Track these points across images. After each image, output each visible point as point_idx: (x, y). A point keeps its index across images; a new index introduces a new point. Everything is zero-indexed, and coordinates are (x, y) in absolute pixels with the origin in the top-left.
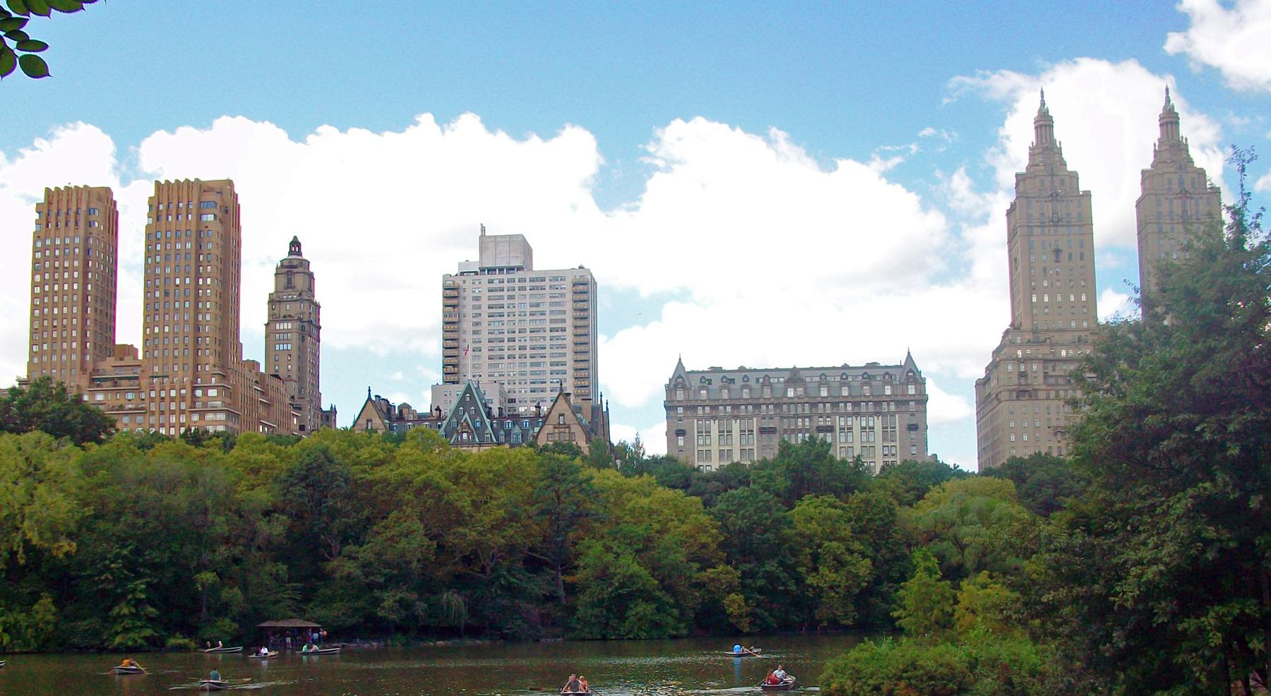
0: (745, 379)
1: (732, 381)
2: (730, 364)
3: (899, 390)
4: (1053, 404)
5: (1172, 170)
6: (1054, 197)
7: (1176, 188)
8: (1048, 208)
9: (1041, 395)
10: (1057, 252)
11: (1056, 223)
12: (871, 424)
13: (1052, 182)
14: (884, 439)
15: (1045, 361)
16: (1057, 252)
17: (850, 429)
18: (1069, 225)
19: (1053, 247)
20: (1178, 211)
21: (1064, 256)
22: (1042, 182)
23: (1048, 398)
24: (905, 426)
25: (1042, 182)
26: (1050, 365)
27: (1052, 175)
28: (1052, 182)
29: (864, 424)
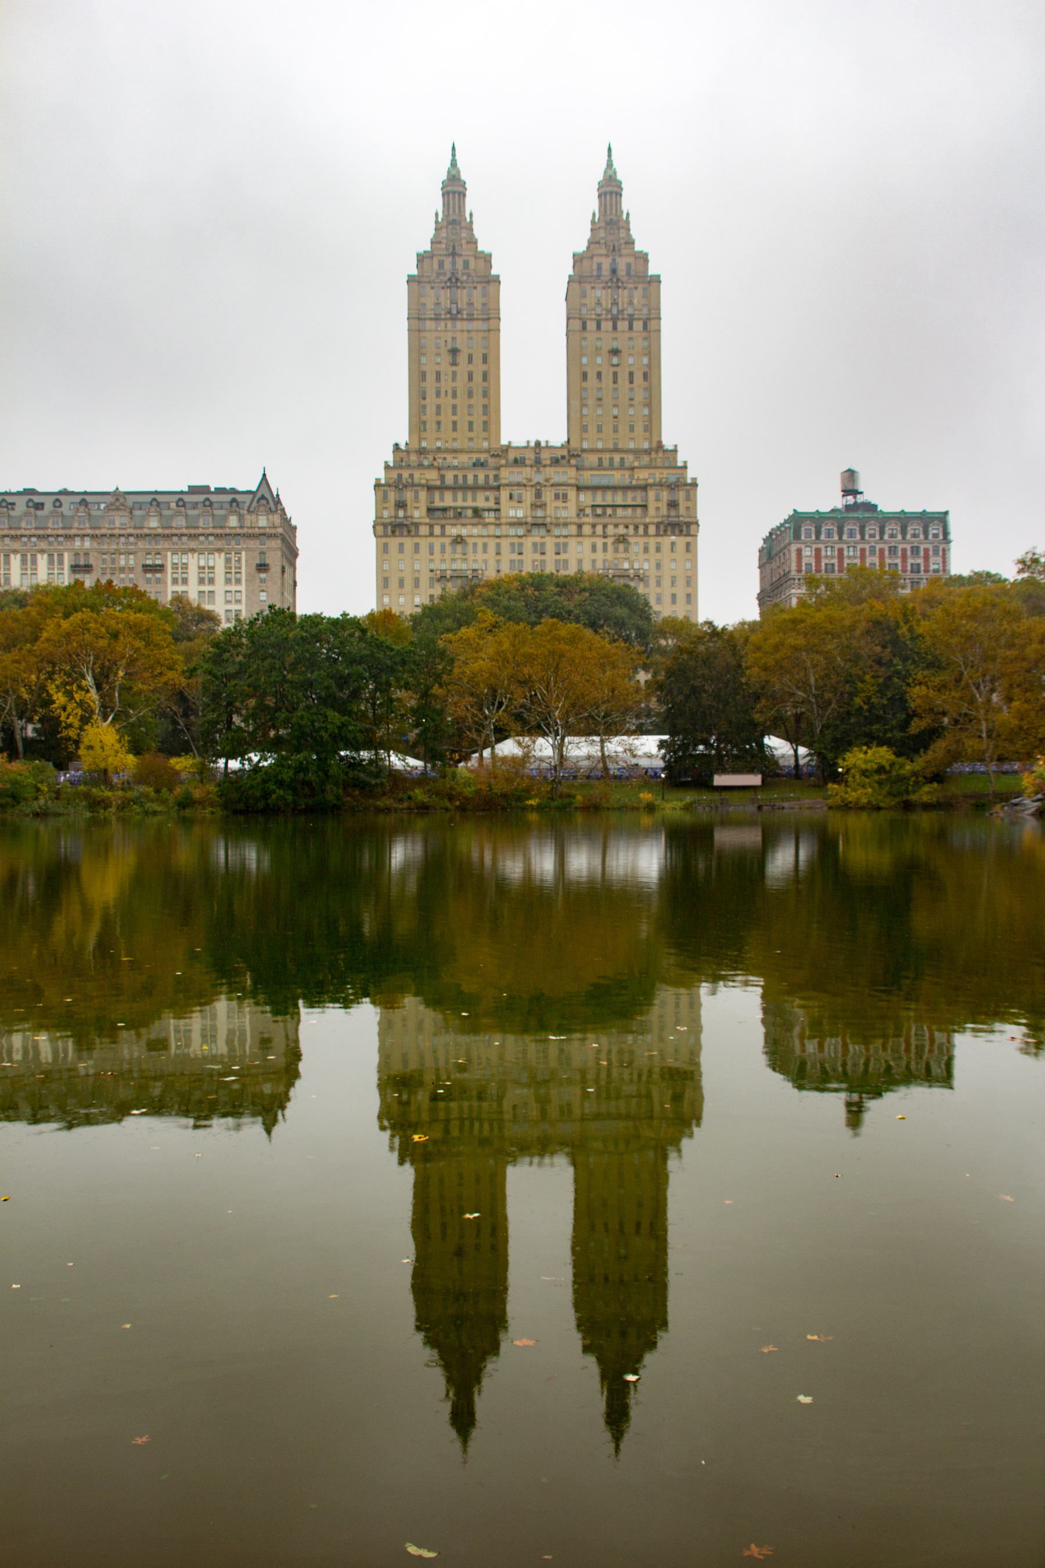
0: (57, 504)
1: (39, 506)
2: (47, 484)
3: (254, 522)
4: (437, 543)
5: (604, 252)
6: (453, 282)
7: (606, 271)
8: (445, 296)
9: (424, 530)
10: (454, 352)
11: (454, 316)
12: (211, 564)
13: (454, 263)
14: (228, 581)
15: (430, 488)
16: (454, 352)
17: (185, 566)
18: (471, 319)
19: (449, 347)
20: (607, 303)
21: (462, 358)
22: (441, 264)
23: (431, 534)
24: (254, 566)
25: (441, 264)
26: (437, 494)
27: (454, 254)
28: (454, 263)
29: (202, 563)
